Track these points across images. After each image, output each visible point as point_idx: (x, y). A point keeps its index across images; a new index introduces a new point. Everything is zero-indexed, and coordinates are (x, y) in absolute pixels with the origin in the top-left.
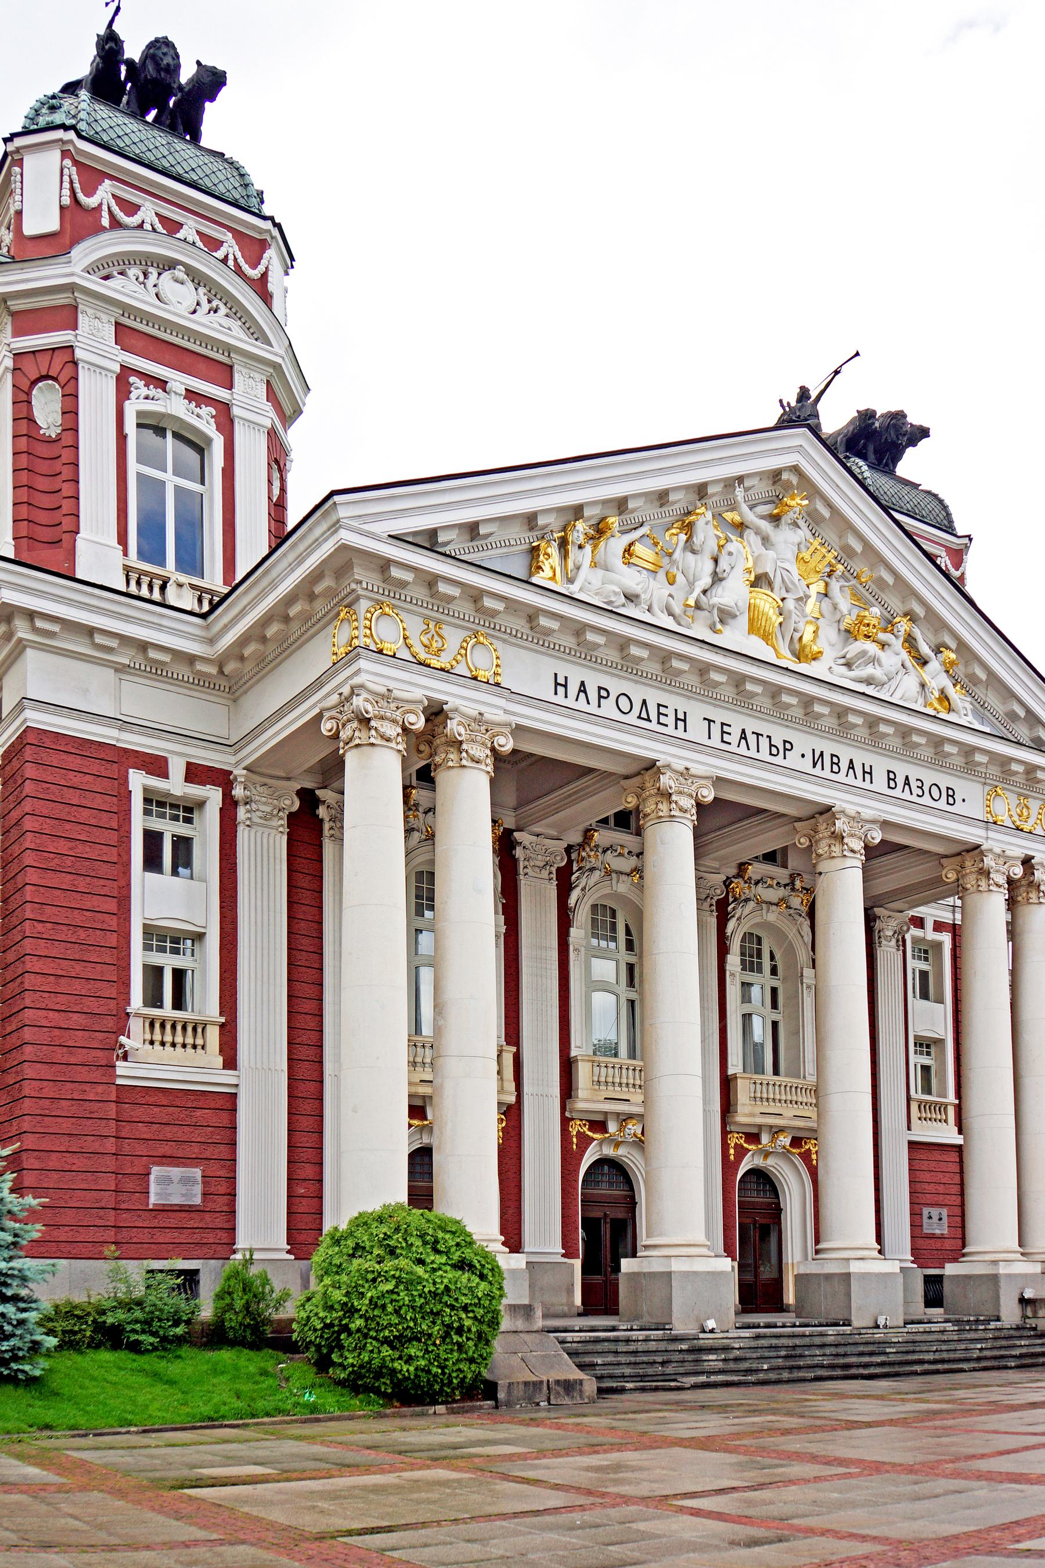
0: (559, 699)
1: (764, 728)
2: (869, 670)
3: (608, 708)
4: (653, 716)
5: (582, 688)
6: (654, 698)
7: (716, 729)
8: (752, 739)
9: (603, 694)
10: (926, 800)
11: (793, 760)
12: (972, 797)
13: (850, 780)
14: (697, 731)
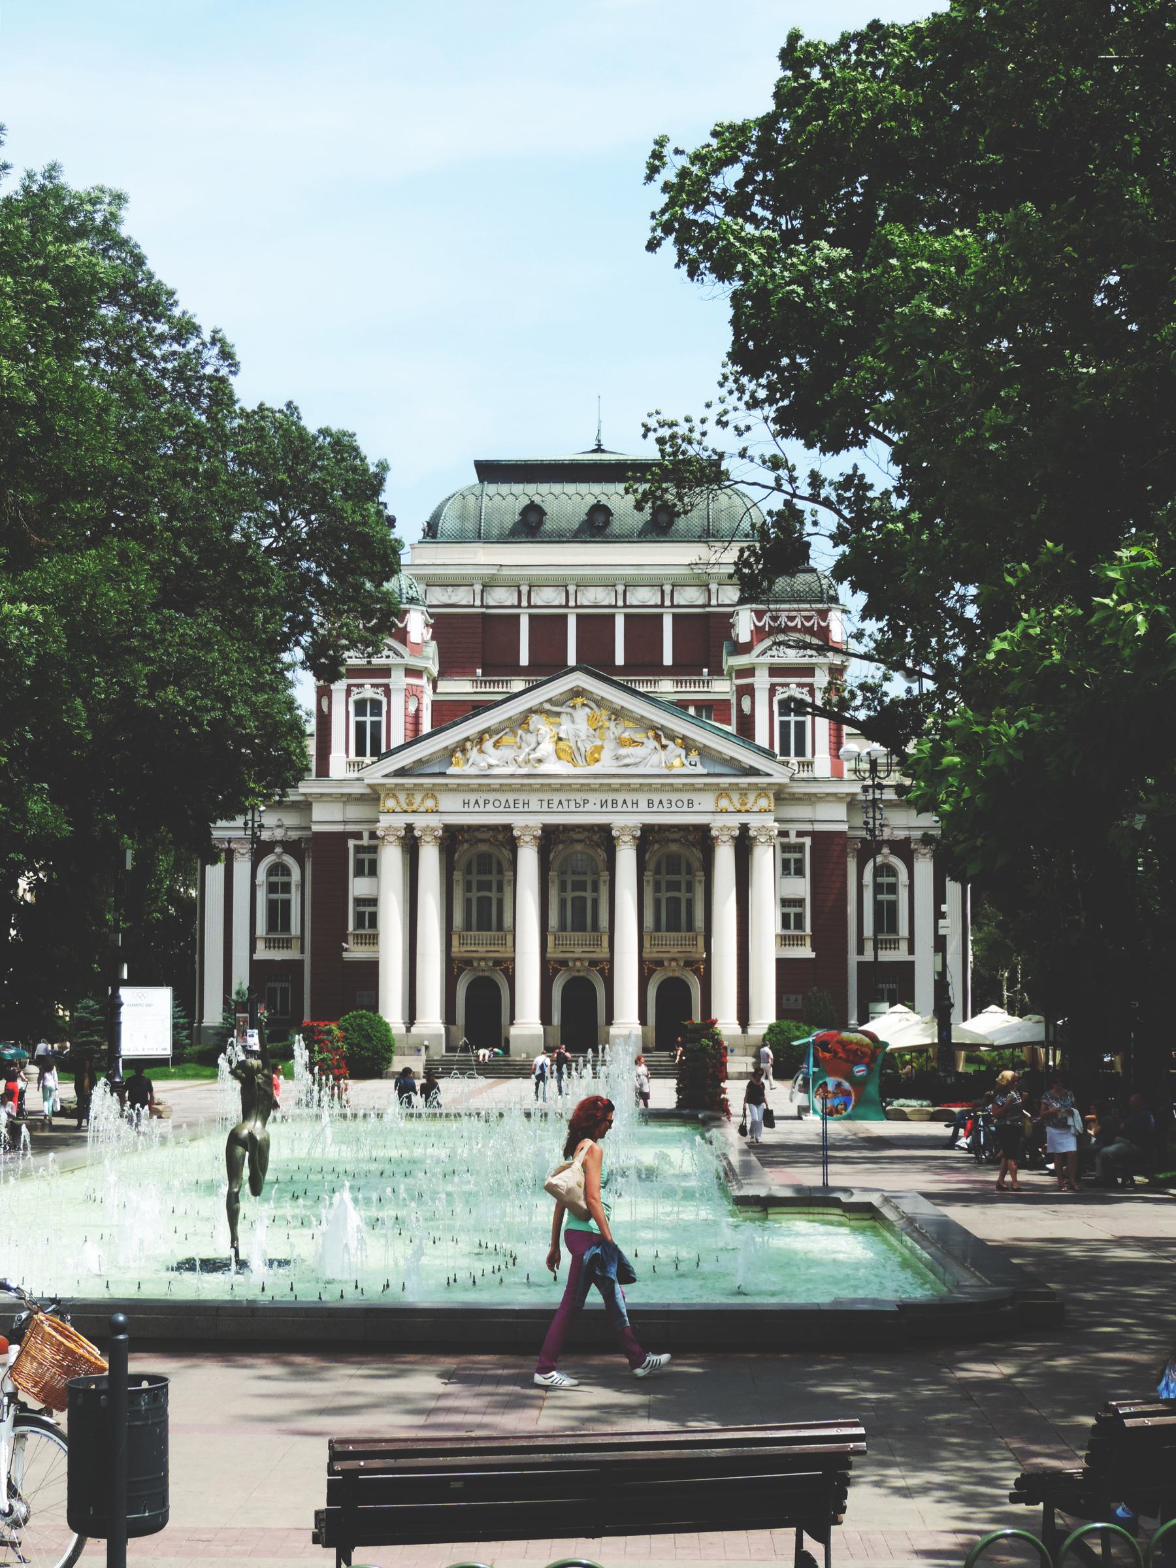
0: (466, 809)
1: (572, 796)
2: (627, 761)
3: (490, 808)
4: (512, 805)
5: (477, 802)
6: (511, 797)
7: (545, 804)
8: (565, 803)
9: (486, 802)
10: (674, 808)
11: (588, 807)
12: (706, 802)
13: (625, 809)
14: (534, 806)
